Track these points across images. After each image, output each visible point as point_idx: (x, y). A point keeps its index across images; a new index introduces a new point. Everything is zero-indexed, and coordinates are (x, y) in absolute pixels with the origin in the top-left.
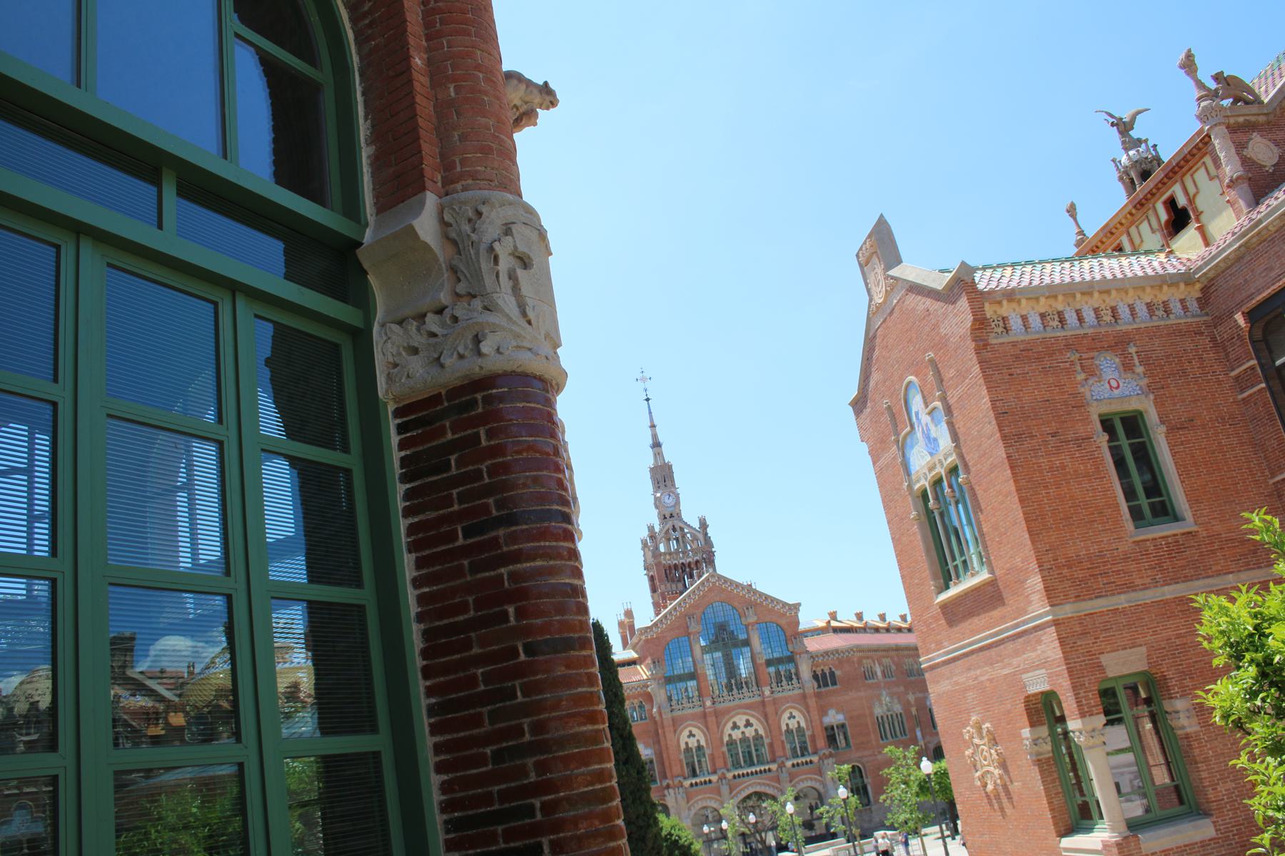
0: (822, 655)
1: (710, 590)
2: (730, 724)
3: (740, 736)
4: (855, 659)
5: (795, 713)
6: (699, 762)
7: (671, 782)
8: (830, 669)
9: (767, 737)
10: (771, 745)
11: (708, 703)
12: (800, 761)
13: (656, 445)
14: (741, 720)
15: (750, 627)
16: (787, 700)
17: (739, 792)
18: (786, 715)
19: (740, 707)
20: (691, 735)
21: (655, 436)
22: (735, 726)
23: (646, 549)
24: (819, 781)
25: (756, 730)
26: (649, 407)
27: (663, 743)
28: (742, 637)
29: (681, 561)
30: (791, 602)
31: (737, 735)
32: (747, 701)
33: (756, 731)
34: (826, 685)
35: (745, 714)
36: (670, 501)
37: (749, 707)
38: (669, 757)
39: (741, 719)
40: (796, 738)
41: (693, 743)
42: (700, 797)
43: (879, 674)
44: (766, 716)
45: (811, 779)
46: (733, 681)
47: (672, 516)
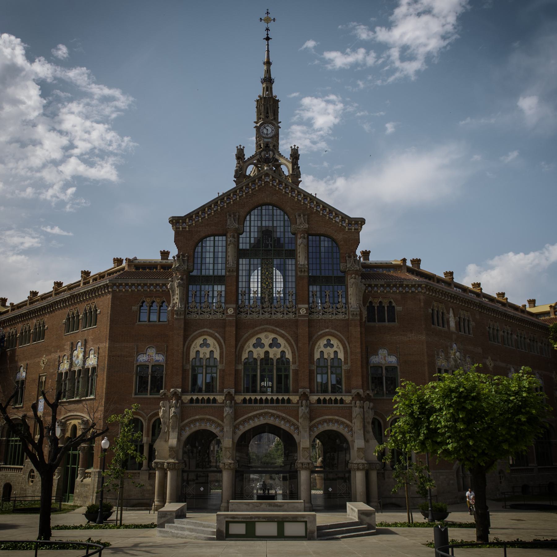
2: (253, 341)
3: (262, 356)
4: (422, 297)
5: (334, 341)
8: (390, 302)
9: (294, 363)
10: (296, 372)
12: (327, 398)
14: (267, 338)
17: (245, 421)
18: (323, 342)
21: (268, 71)
22: (259, 344)
26: (268, 45)
32: (279, 316)
33: (283, 352)
34: (382, 320)
35: (273, 332)
37: (280, 324)
39: (267, 337)
41: (205, 354)
42: (197, 417)
43: (452, 324)
45: (337, 421)
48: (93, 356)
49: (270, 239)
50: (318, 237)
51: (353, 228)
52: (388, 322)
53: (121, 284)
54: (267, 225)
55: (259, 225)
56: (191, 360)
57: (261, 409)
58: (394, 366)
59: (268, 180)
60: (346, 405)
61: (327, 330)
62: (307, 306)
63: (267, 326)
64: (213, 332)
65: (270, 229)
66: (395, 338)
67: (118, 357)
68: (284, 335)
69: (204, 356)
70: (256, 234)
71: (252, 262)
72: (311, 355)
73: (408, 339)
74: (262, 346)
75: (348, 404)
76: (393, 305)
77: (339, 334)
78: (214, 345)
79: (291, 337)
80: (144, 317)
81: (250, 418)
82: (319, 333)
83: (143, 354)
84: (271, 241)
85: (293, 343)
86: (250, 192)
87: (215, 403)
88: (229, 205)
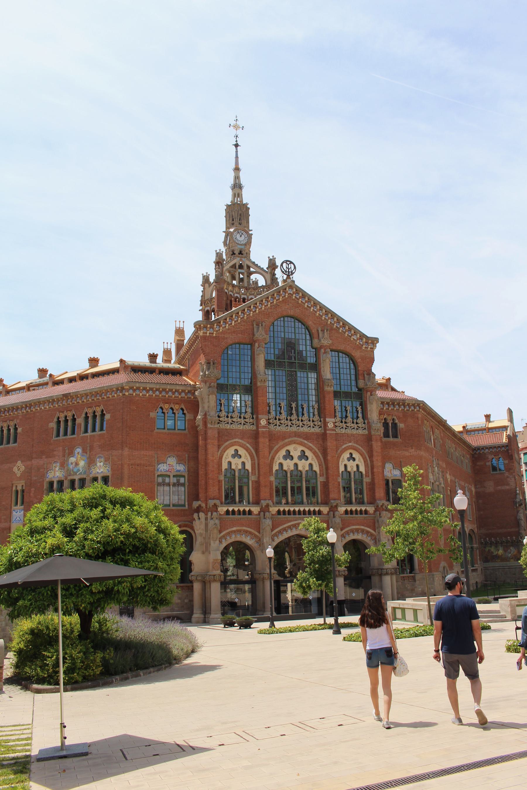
0: (388, 403)
1: (285, 301)
2: (283, 452)
3: (292, 468)
6: (241, 488)
7: (203, 505)
8: (393, 419)
10: (325, 485)
11: (263, 422)
13: (237, 187)
14: (296, 451)
15: (323, 350)
16: (349, 438)
17: (280, 532)
18: (346, 455)
19: (297, 434)
20: (236, 455)
21: (237, 178)
22: (288, 456)
23: (207, 285)
24: (372, 535)
25: (311, 465)
26: (237, 152)
27: (201, 457)
28: (311, 360)
29: (243, 296)
30: (369, 334)
31: (288, 465)
32: (305, 429)
35: (301, 444)
36: (241, 239)
37: (307, 437)
38: (206, 474)
39: (295, 449)
40: (353, 483)
41: (237, 464)
42: (235, 529)
44: (325, 453)
45: (363, 531)
46: (294, 405)
47: (240, 253)
48: (102, 464)
49: (293, 351)
50: (337, 353)
51: (370, 347)
52: (393, 437)
53: (138, 388)
54: (290, 337)
55: (283, 336)
56: (223, 470)
57: (295, 520)
58: (398, 479)
59: (291, 292)
60: (370, 516)
61: (350, 444)
62: (333, 420)
63: (296, 438)
64: (245, 443)
65: (293, 341)
66: (399, 452)
67: (138, 465)
68: (312, 447)
69: (237, 466)
70: (280, 345)
71: (277, 373)
72: (338, 468)
73: (409, 454)
74: (292, 458)
75: (372, 514)
76: (396, 422)
77: (360, 448)
78: (246, 456)
79: (319, 450)
80: (159, 424)
81: (285, 530)
82: (343, 447)
83: (164, 463)
84: (295, 353)
85: (321, 456)
86: (275, 303)
87: (251, 515)
88: (255, 313)
